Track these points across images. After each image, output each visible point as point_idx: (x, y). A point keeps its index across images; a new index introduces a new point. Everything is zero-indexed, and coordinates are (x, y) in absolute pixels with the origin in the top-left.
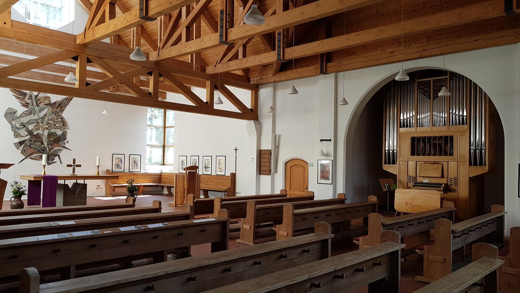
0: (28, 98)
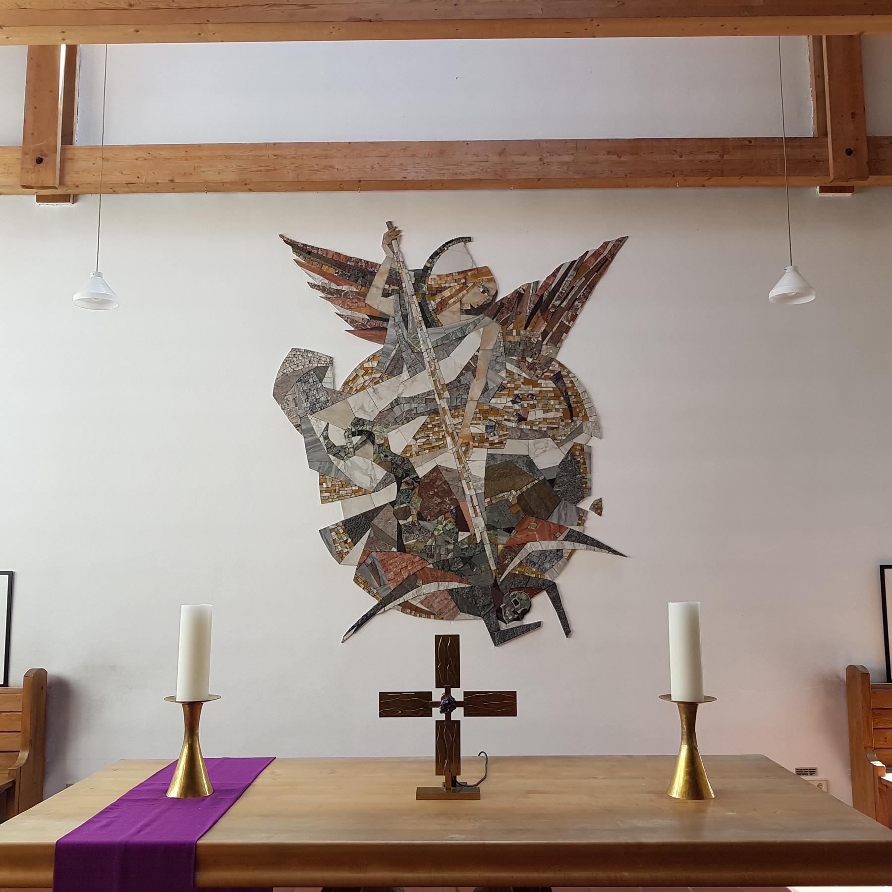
0: (381, 292)
